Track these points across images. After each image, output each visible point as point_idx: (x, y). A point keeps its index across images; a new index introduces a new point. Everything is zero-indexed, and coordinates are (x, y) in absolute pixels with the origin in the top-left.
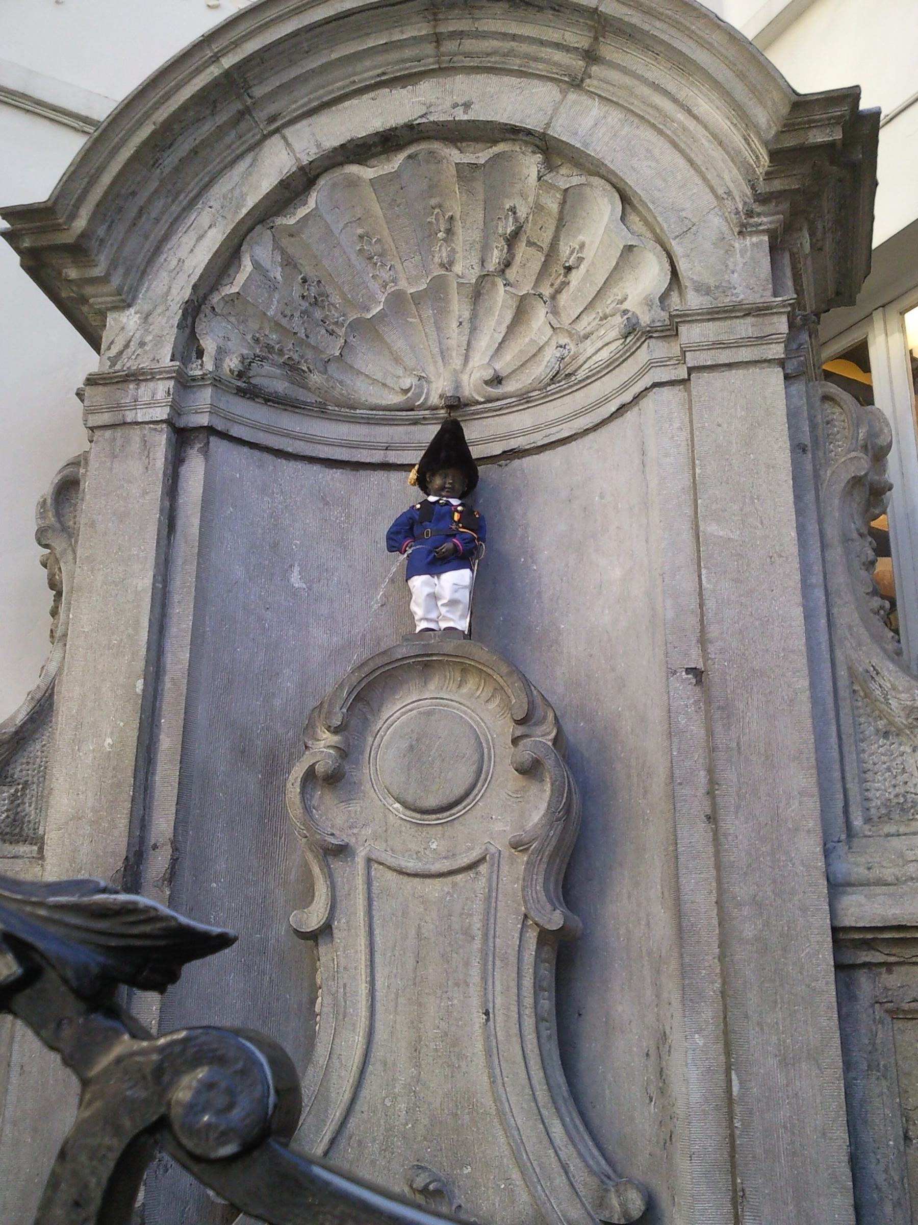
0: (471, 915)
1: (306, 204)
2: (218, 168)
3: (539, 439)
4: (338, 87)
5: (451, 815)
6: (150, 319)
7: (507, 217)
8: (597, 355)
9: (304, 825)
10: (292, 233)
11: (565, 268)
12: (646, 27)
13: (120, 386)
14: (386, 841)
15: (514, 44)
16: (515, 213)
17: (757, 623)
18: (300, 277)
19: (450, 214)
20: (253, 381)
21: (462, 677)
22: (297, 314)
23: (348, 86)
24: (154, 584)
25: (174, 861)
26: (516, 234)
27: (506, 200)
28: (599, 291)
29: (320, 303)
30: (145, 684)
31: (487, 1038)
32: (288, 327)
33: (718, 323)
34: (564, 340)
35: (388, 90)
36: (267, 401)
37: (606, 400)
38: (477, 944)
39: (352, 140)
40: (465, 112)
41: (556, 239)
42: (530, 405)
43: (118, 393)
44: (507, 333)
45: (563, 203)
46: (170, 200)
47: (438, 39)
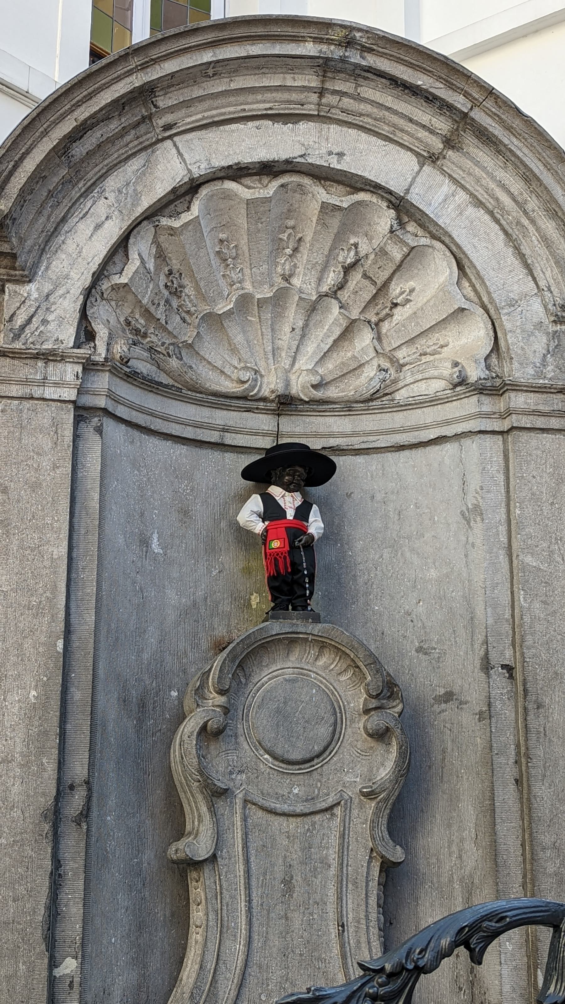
0: (328, 848)
1: (189, 208)
2: (115, 162)
3: (356, 442)
4: (230, 111)
5: (311, 766)
6: (52, 298)
7: (349, 250)
8: (415, 385)
9: (198, 772)
11: (393, 303)
12: (506, 141)
13: (28, 361)
14: (257, 786)
15: (387, 114)
16: (356, 248)
17: (559, 637)
18: (166, 269)
19: (300, 235)
21: (319, 652)
22: (162, 303)
23: (239, 112)
25: (89, 798)
26: (353, 265)
27: (351, 236)
28: (422, 333)
29: (179, 294)
31: (342, 946)
32: (154, 314)
33: (537, 395)
34: (386, 364)
35: (270, 123)
37: (426, 427)
38: (333, 871)
39: (239, 163)
40: (339, 162)
41: (390, 279)
42: (351, 413)
44: (332, 345)
47: (322, 92)
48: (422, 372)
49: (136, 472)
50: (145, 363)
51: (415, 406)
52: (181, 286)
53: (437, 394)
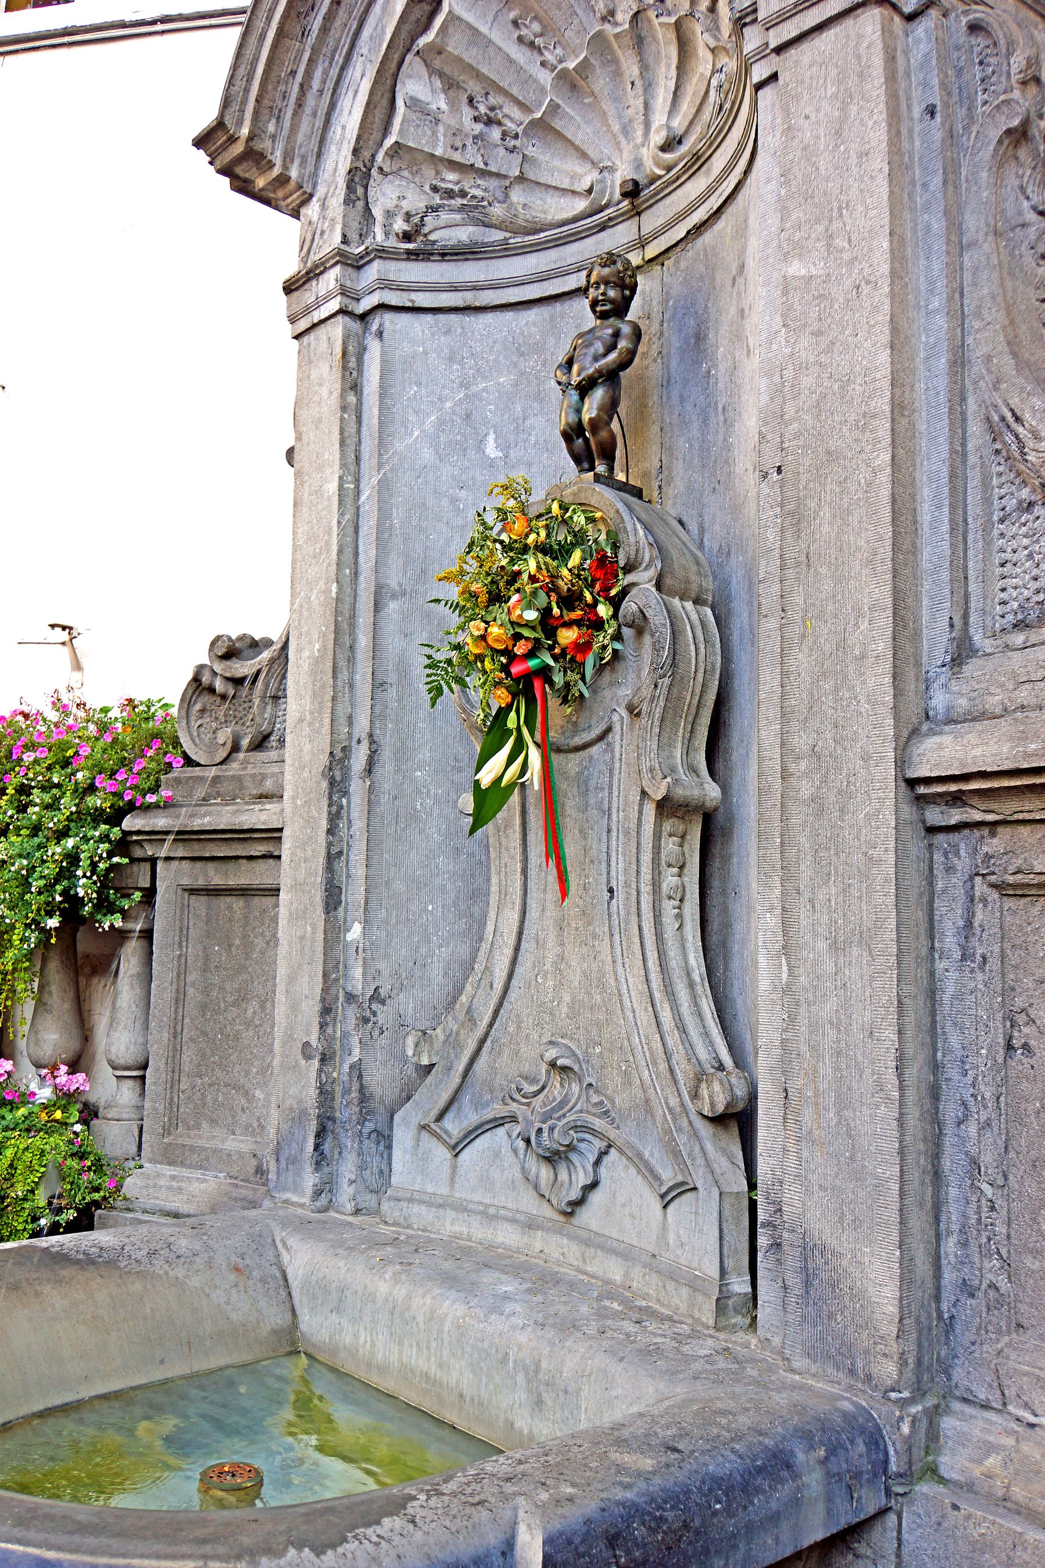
3: (715, 202)
10: (437, 50)
20: (432, 237)
22: (469, 142)
24: (341, 487)
30: (340, 588)
36: (443, 255)
43: (307, 294)
46: (327, 64)
49: (456, 367)
50: (463, 228)
52: (492, 109)
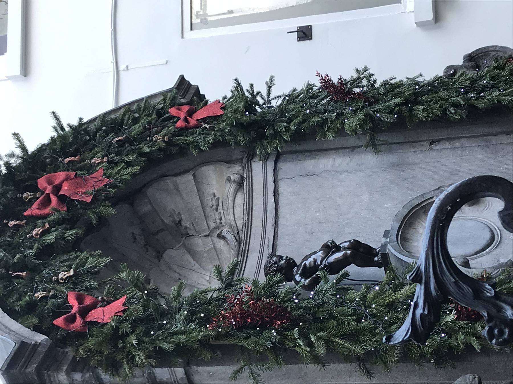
5: (496, 229)
7: (135, 238)
37: (266, 204)
41: (162, 220)
42: (246, 252)
44: (197, 262)
45: (150, 203)
48: (228, 209)
51: (251, 211)
53: (245, 192)
